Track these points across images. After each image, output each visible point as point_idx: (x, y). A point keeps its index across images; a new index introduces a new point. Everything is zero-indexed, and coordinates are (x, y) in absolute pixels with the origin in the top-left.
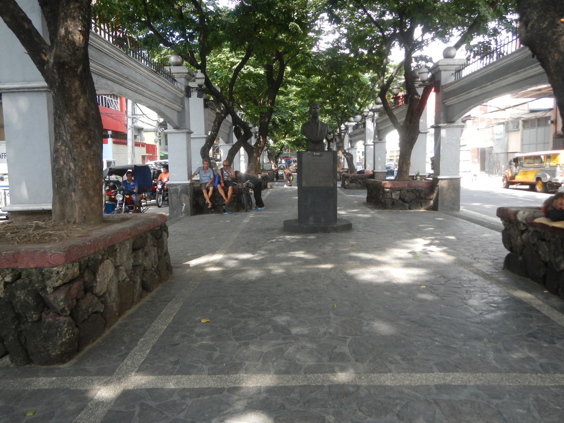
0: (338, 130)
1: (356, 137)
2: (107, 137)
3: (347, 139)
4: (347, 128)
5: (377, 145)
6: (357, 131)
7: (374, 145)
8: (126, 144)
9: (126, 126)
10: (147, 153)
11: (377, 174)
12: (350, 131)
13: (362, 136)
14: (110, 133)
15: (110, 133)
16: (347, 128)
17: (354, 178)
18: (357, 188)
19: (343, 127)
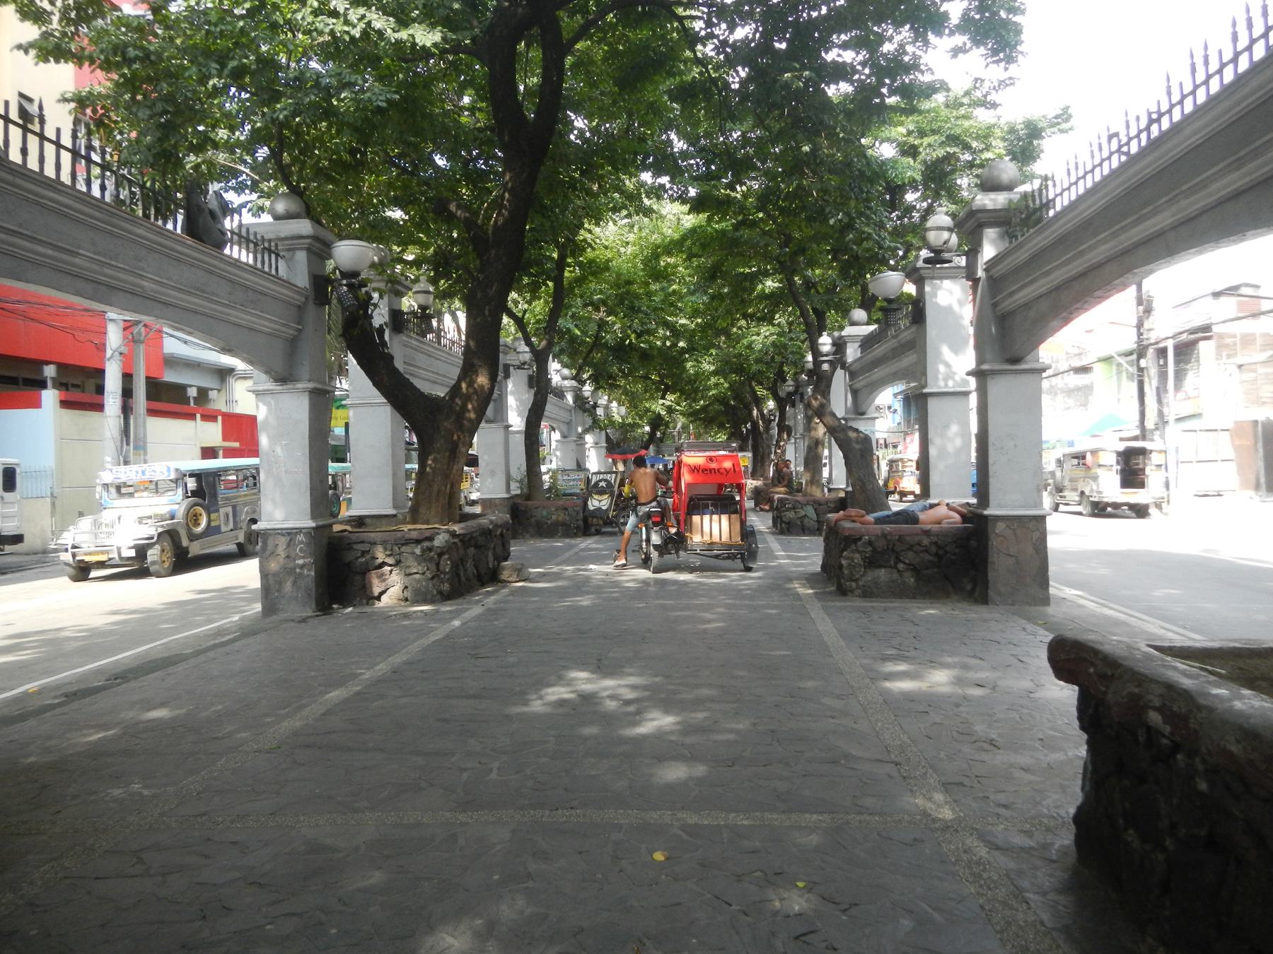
0: (810, 358)
1: (878, 373)
2: (42, 385)
3: (840, 380)
4: (839, 345)
5: (995, 387)
6: (879, 350)
7: (982, 391)
8: (99, 407)
9: (102, 348)
10: (224, 440)
11: (1000, 527)
12: (852, 353)
13: (909, 359)
14: (50, 371)
15: (50, 371)
16: (839, 345)
17: (881, 544)
18: (898, 592)
19: (825, 342)
